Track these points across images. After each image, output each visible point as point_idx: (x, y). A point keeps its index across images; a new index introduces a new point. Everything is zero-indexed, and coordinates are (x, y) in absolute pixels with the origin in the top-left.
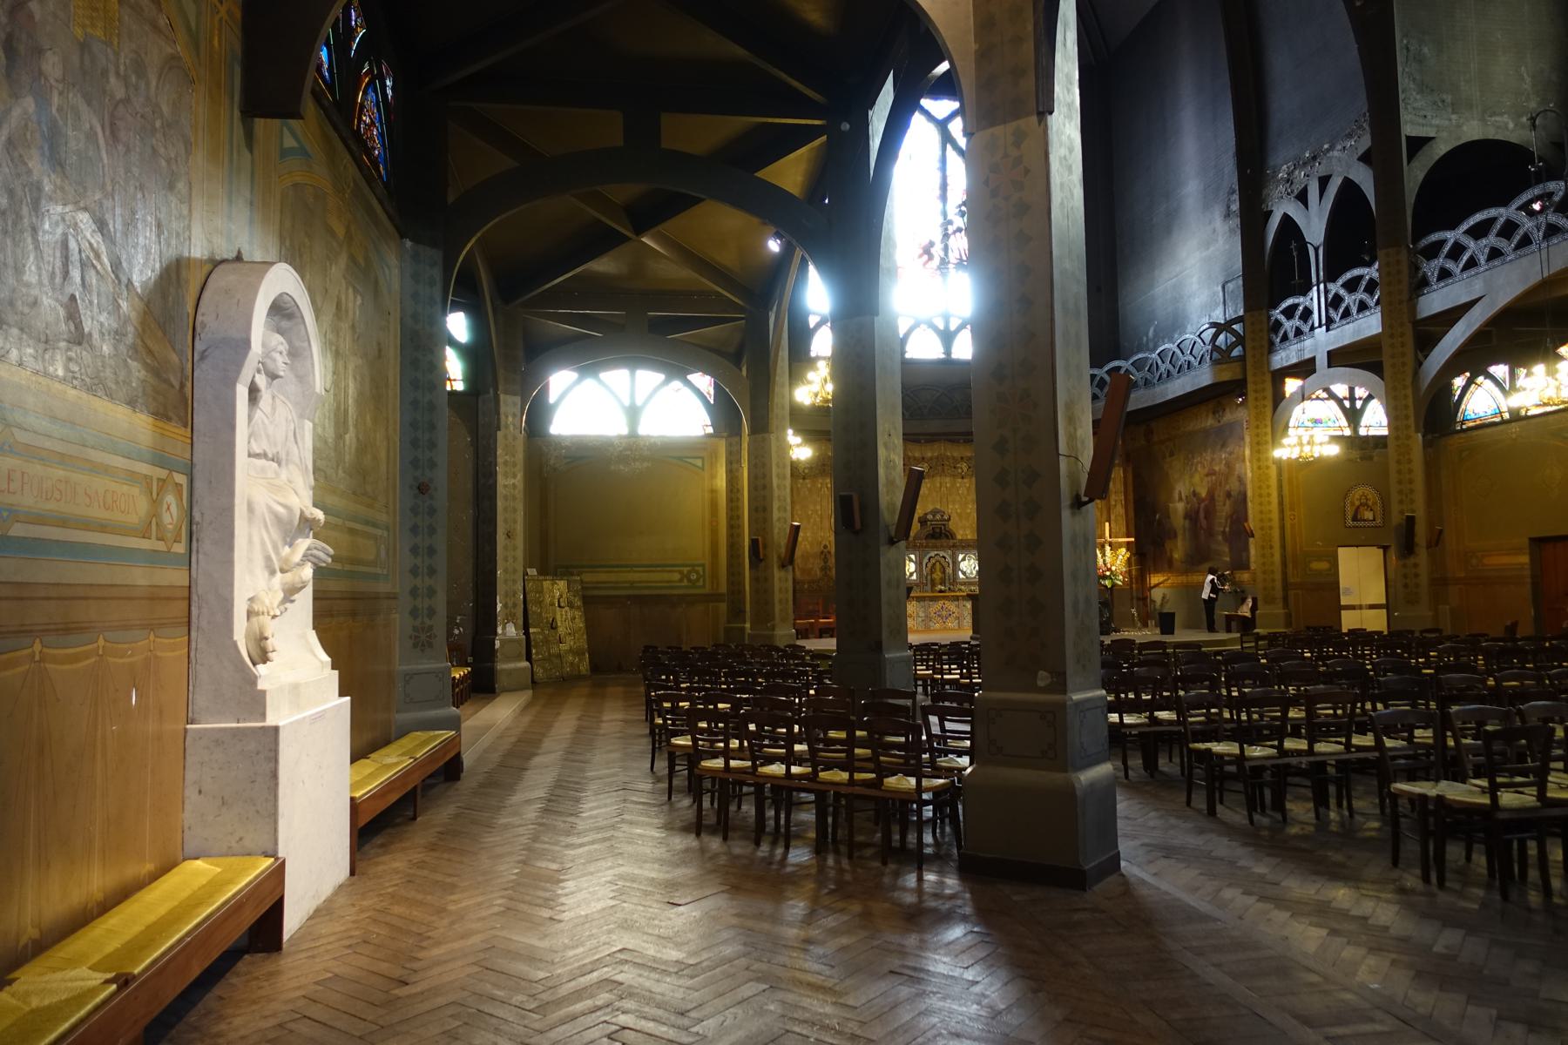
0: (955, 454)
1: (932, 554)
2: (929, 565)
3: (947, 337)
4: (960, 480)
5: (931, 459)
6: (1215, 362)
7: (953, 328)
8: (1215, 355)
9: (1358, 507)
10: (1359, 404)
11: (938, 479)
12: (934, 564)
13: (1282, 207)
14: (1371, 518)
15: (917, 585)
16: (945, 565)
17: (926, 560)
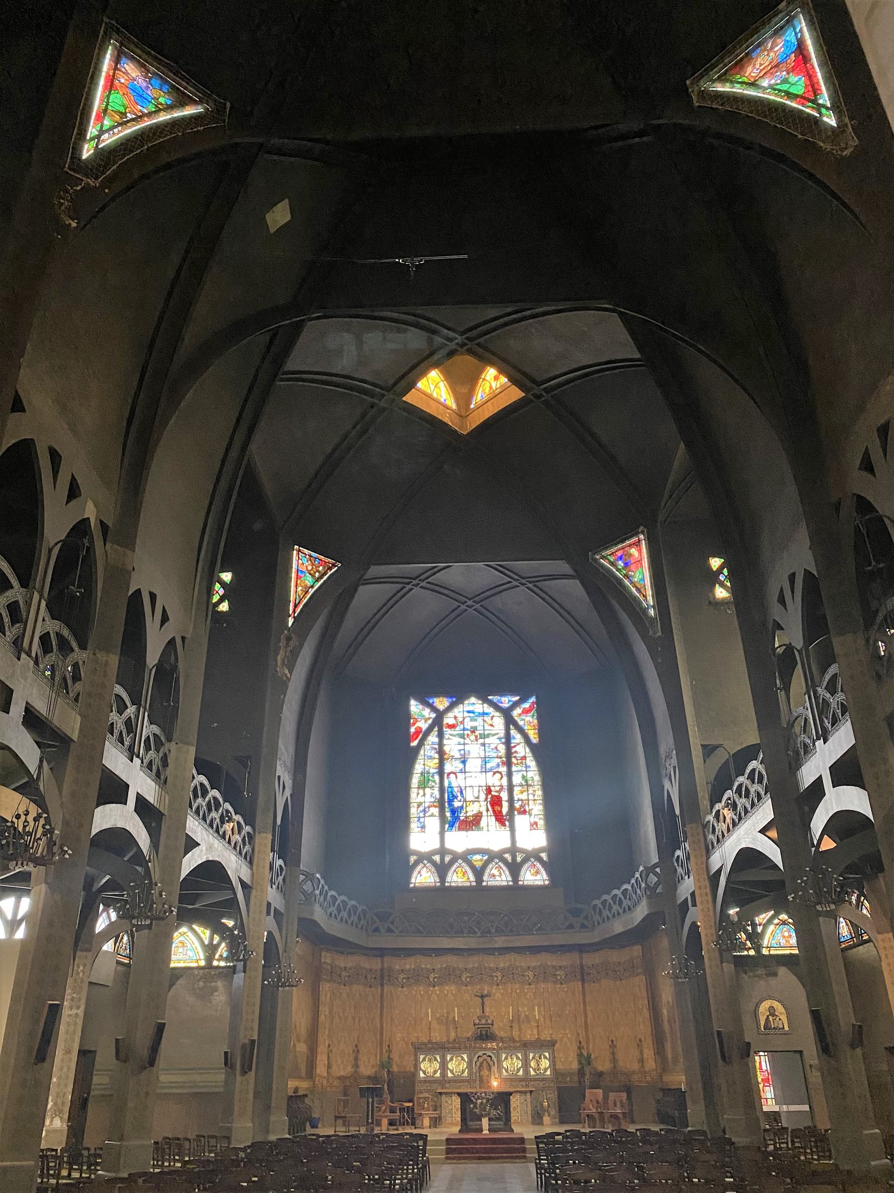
0: (523, 964)
1: (480, 1053)
2: (478, 1064)
3: (515, 869)
4: (527, 986)
5: (504, 968)
6: (649, 897)
7: (519, 859)
8: (648, 893)
9: (768, 1016)
10: (760, 929)
11: (509, 986)
12: (482, 1063)
13: (667, 785)
14: (781, 1026)
15: (468, 1081)
16: (491, 1063)
17: (475, 1059)
